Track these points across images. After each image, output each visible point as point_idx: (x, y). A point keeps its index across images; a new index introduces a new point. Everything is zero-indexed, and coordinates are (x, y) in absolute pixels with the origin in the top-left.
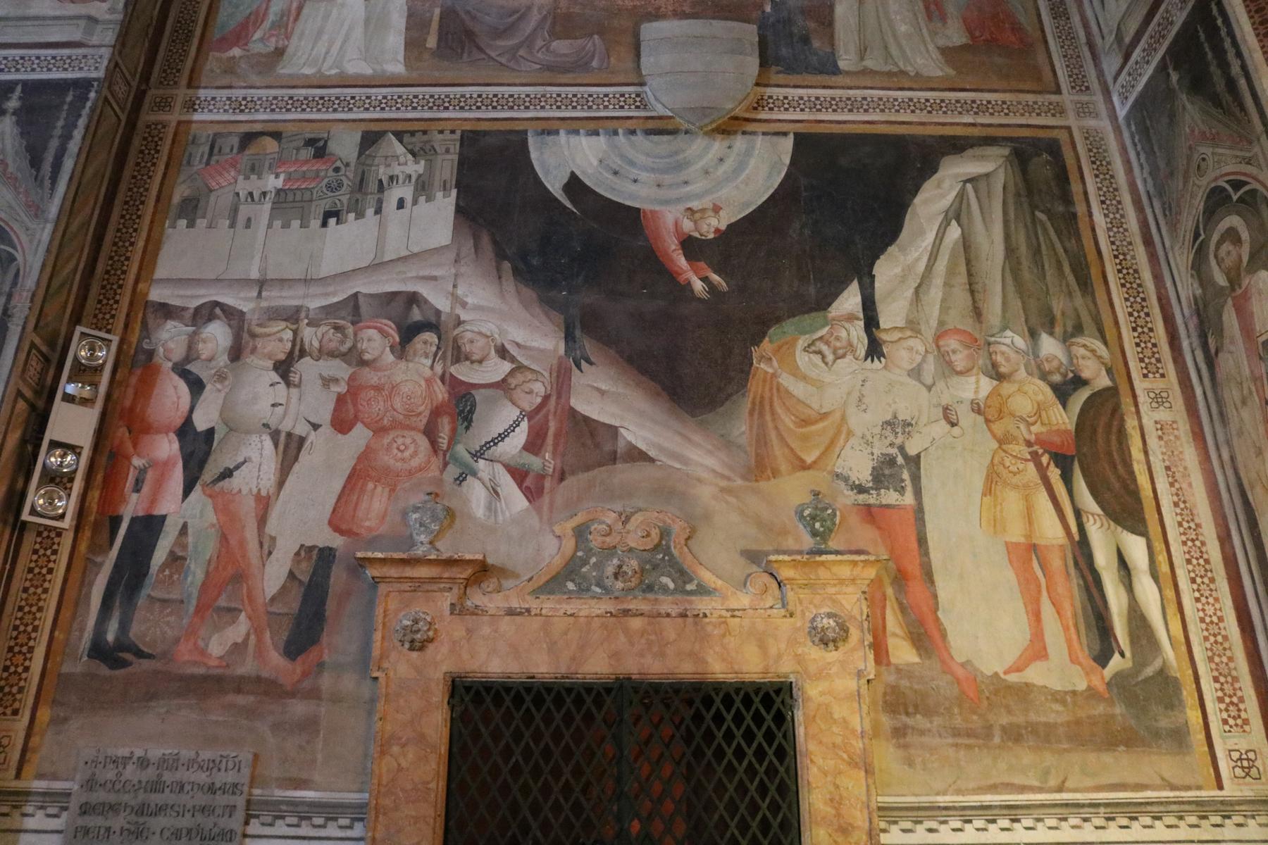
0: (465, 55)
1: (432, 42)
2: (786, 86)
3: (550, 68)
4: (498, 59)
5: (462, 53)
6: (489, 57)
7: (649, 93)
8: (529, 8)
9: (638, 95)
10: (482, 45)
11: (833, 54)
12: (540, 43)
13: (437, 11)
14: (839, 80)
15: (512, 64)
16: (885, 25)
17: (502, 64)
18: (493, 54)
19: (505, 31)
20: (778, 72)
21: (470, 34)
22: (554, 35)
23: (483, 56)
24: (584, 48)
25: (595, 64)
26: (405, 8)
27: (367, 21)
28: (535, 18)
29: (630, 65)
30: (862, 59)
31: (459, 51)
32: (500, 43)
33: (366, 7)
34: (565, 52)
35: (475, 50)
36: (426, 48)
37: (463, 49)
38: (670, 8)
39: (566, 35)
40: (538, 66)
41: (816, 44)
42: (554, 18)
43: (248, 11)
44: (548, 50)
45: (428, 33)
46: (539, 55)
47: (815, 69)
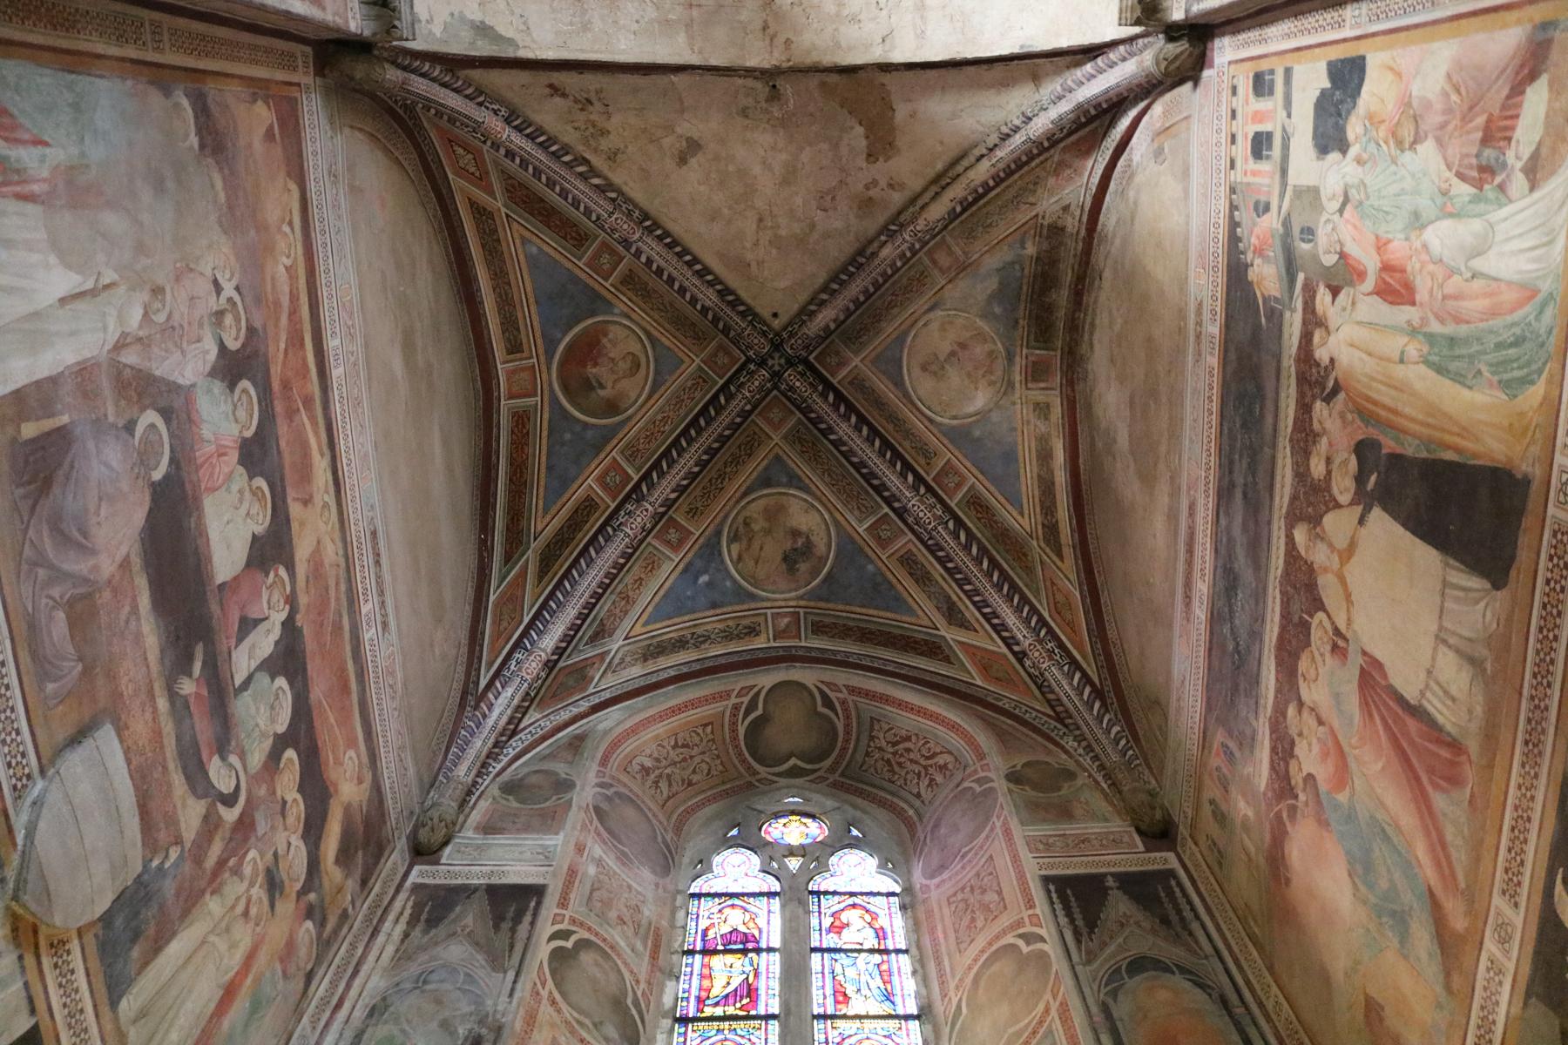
0: (21, 491)
1: (29, 430)
2: (85, 960)
3: (33, 627)
4: (27, 542)
5: (23, 485)
6: (27, 528)
7: (36, 792)
8: (93, 552)
9: (29, 777)
10: (38, 508)
11: (131, 982)
12: (56, 592)
13: (65, 419)
14: (105, 1010)
15: (25, 567)
16: (171, 1014)
17: (21, 554)
18: (31, 533)
19: (62, 533)
20: (96, 936)
21: (47, 484)
22: (70, 605)
23: (25, 519)
24: (65, 659)
25: (50, 687)
26: (61, 369)
27: (36, 315)
28: (80, 566)
29: (61, 736)
30: (135, 1022)
31: (25, 478)
32: (46, 533)
33: (51, 306)
34: (55, 638)
35: (30, 502)
36: (19, 426)
37: (29, 483)
38: (130, 742)
39: (72, 623)
40: (30, 610)
41: (135, 953)
42: (90, 594)
43: (15, 111)
44: (53, 607)
45: (38, 419)
46: (44, 601)
47: (111, 977)
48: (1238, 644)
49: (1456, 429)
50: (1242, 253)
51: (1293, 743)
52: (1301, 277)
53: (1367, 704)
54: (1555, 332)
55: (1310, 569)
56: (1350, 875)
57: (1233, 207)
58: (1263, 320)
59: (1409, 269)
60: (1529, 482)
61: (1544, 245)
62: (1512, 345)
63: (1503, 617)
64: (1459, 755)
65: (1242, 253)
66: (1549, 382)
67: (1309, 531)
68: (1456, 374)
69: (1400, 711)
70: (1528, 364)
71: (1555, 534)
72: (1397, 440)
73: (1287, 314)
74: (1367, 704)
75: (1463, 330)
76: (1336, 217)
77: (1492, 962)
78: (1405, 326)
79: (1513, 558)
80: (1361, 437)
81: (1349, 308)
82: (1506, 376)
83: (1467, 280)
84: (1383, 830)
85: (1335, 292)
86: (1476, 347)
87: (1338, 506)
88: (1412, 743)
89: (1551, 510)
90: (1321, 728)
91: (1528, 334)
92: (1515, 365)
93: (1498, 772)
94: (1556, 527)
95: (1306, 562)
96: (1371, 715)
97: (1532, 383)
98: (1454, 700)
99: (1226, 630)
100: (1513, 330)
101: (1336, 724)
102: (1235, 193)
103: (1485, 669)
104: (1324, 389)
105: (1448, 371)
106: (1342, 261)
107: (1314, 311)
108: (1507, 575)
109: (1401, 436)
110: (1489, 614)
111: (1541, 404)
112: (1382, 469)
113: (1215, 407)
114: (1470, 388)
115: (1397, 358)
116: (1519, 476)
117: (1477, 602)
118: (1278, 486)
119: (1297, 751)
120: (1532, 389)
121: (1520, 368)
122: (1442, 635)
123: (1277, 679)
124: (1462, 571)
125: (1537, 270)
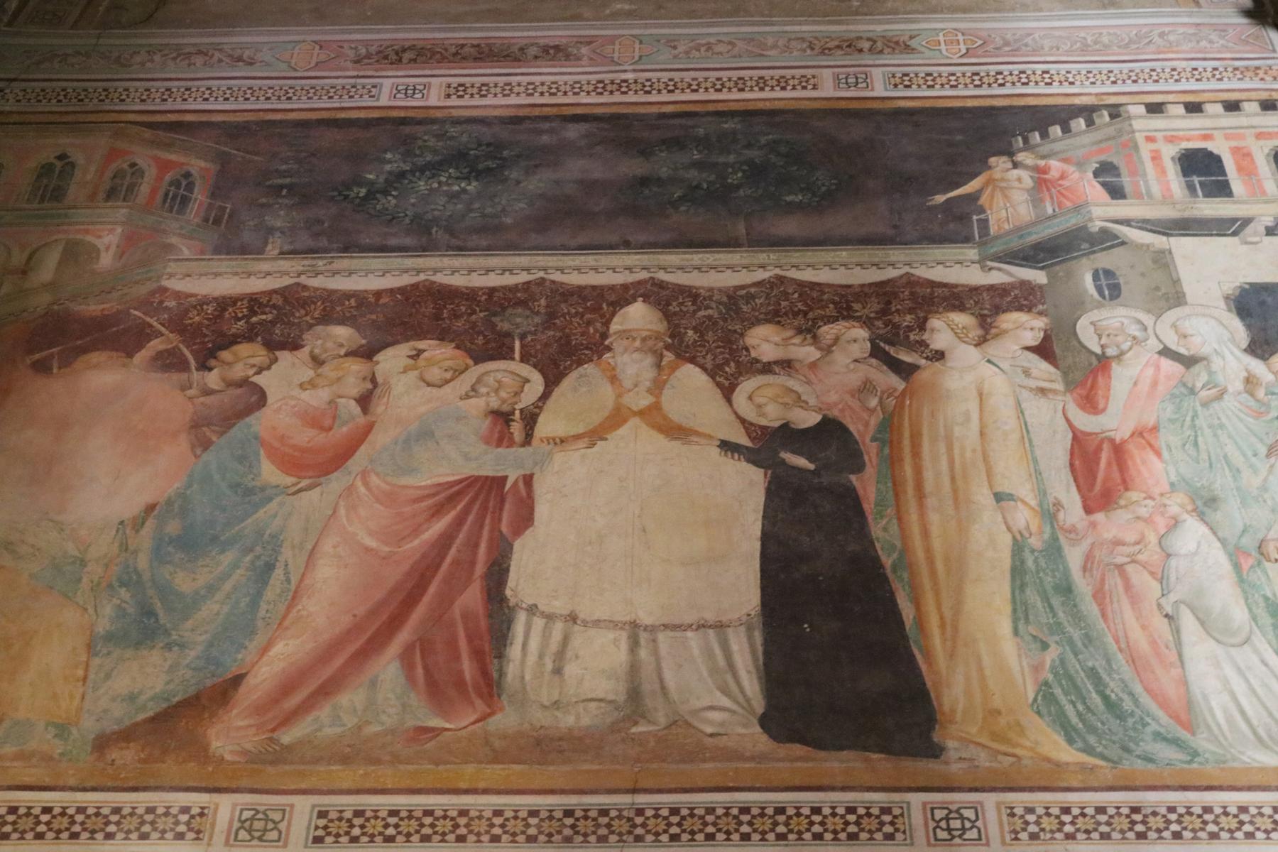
48: (386, 193)
49: (948, 614)
50: (1026, 140)
51: (295, 346)
52: (1037, 276)
53: (452, 500)
54: (1151, 766)
55: (598, 348)
56: (150, 508)
57: (1088, 112)
58: (940, 199)
59: (1134, 495)
60: (936, 756)
61: (1255, 733)
62: (1105, 698)
63: (723, 741)
64: (481, 696)
65: (1026, 140)
66: (1083, 767)
67: (658, 337)
68: (1025, 604)
69: (480, 569)
70: (1092, 730)
71: (886, 811)
72: (880, 503)
73: (972, 253)
74: (452, 500)
75: (1090, 608)
76: (1153, 344)
77: (202, 815)
78: (1051, 500)
79: (819, 745)
80: (852, 428)
81: (1033, 384)
82: (1057, 691)
83: (1160, 606)
84: (270, 567)
85: (1044, 350)
86: (1076, 635)
87: (728, 393)
88: (446, 600)
89: (916, 799)
90: (355, 409)
91: (1130, 721)
92: (1080, 707)
93: (495, 773)
94: (897, 812)
95: (604, 336)
96: (438, 511)
97: (1070, 741)
98: (558, 671)
99: (394, 162)
100: (1125, 697)
101: (380, 439)
102: (1112, 116)
103: (636, 723)
104: (892, 344)
105: (1023, 587)
106: (1095, 362)
107: (998, 310)
108: (791, 740)
109: (890, 511)
110: (716, 716)
111: (1048, 760)
112: (825, 480)
113: (754, 96)
114: (1016, 632)
115: (999, 489)
116: (936, 737)
117: (725, 692)
118: (697, 258)
119: (285, 357)
120: (1061, 741)
121: (1079, 715)
122: (644, 637)
123: (378, 294)
124: (755, 659)
125: (1219, 725)
